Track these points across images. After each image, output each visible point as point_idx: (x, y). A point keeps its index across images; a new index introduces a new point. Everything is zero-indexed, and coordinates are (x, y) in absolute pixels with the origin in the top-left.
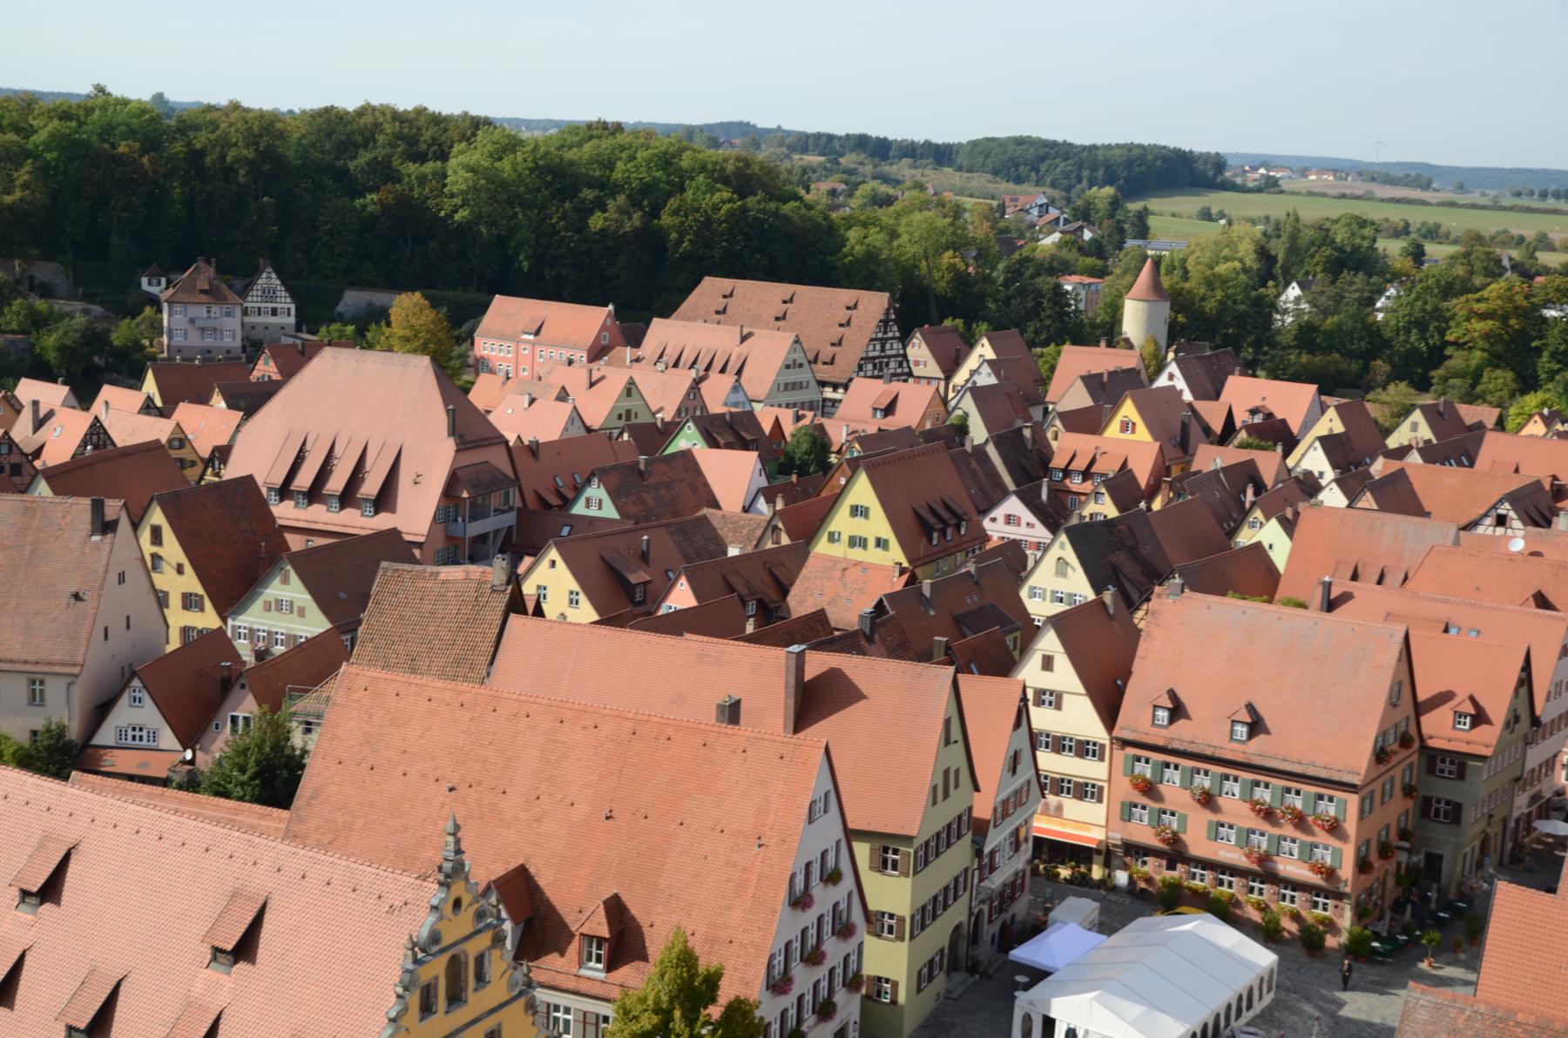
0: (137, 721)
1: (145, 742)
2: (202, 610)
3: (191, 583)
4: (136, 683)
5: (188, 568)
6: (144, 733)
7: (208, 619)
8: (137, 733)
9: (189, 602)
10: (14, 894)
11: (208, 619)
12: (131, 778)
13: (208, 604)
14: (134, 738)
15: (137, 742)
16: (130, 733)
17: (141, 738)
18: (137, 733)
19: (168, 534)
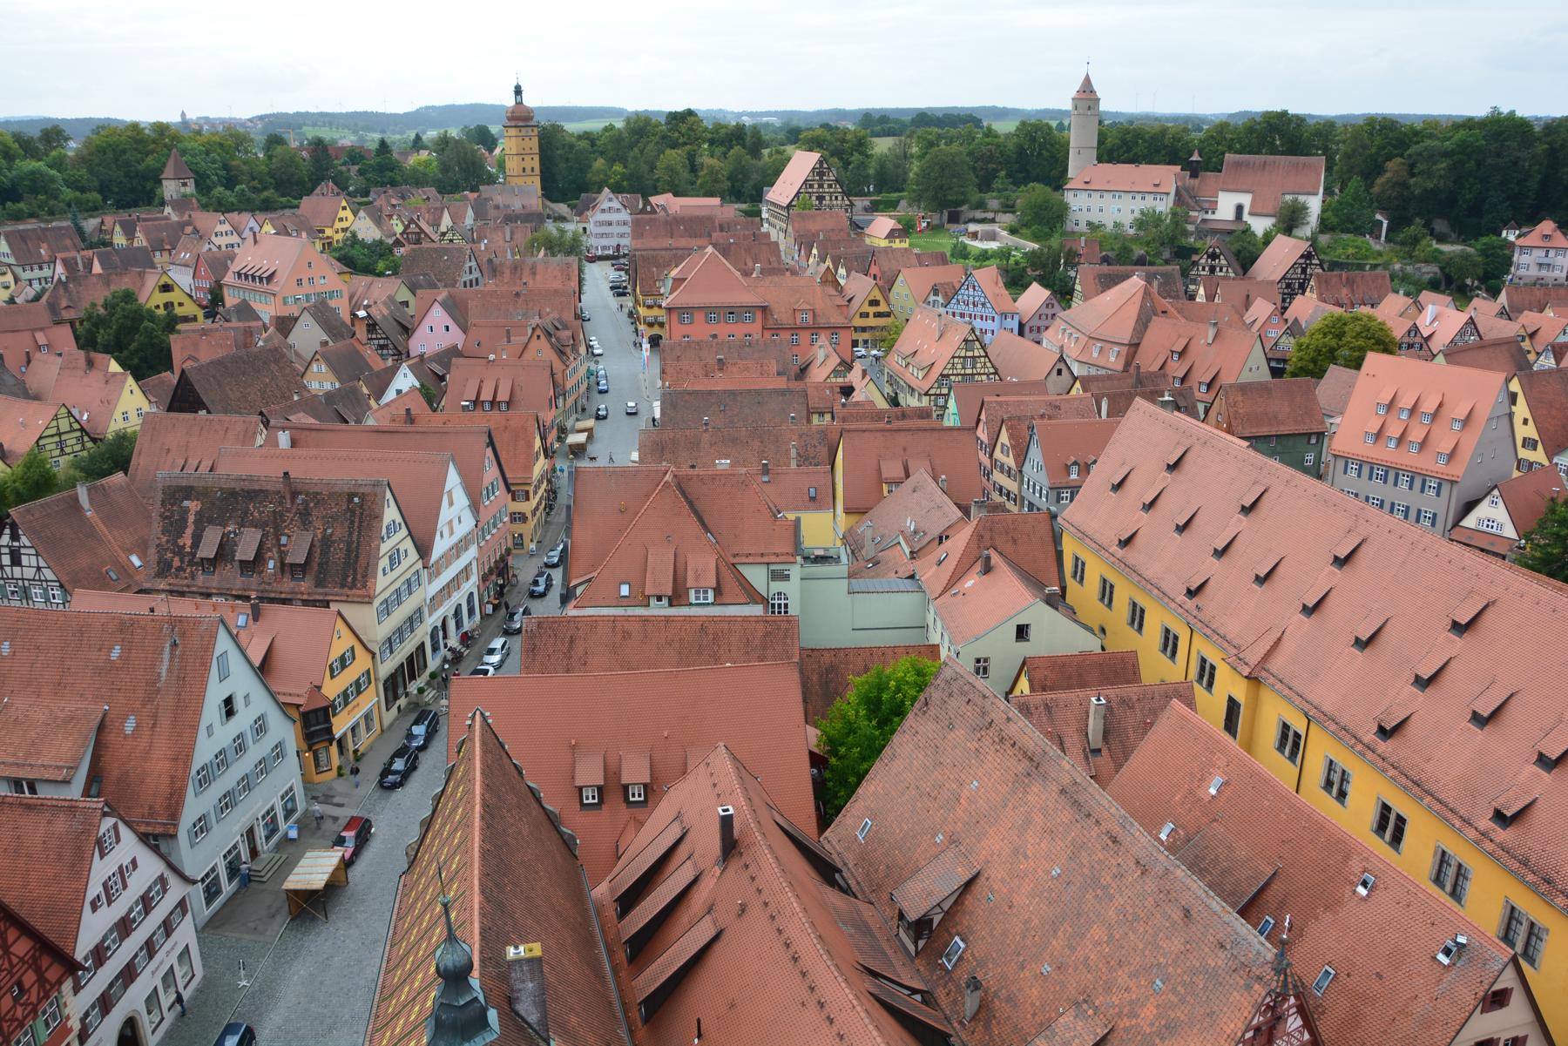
0: (1492, 516)
1: (1494, 529)
2: (1535, 449)
3: (1530, 431)
4: (1496, 492)
5: (1531, 422)
6: (1495, 525)
7: (1538, 456)
8: (1490, 524)
9: (1529, 443)
10: (1447, 623)
11: (1538, 456)
12: (1482, 550)
13: (1540, 446)
14: (1488, 526)
15: (1489, 529)
16: (1486, 523)
17: (1492, 527)
18: (1490, 524)
19: (1521, 399)
